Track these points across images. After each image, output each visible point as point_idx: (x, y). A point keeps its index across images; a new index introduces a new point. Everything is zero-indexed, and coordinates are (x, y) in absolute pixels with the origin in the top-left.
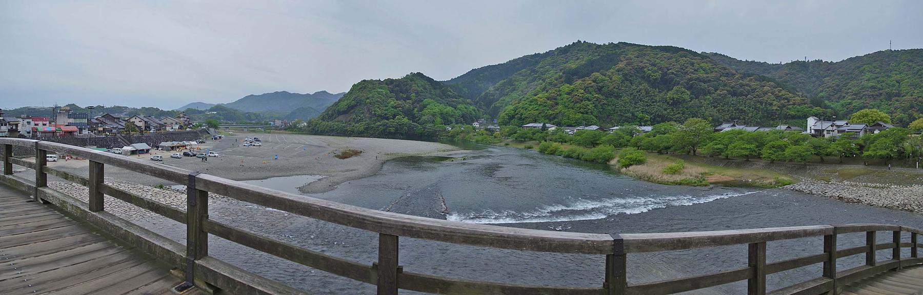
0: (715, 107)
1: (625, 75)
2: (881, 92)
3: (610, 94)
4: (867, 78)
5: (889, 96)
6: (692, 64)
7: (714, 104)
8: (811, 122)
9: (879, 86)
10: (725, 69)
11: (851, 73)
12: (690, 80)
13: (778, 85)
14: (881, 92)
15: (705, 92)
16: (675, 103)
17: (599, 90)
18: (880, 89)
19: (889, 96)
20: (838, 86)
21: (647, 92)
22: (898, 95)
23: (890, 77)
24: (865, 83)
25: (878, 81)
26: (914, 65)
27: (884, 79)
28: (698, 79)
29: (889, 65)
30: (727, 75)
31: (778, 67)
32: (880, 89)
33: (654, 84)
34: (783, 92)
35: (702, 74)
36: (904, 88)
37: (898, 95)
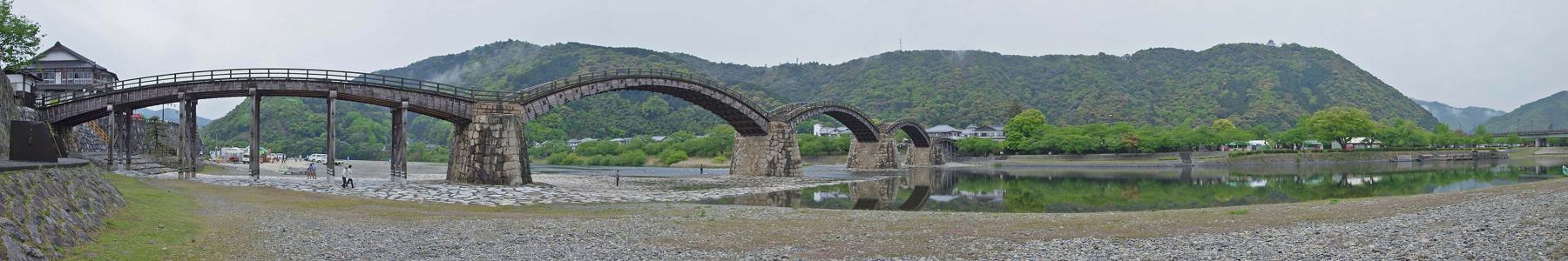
0: (698, 120)
2: (889, 102)
4: (872, 86)
9: (887, 95)
11: (854, 80)
14: (889, 102)
18: (888, 99)
20: (838, 95)
23: (900, 83)
24: (870, 91)
25: (886, 89)
26: (928, 70)
27: (893, 87)
29: (899, 69)
32: (888, 99)
36: (916, 97)
37: (909, 105)
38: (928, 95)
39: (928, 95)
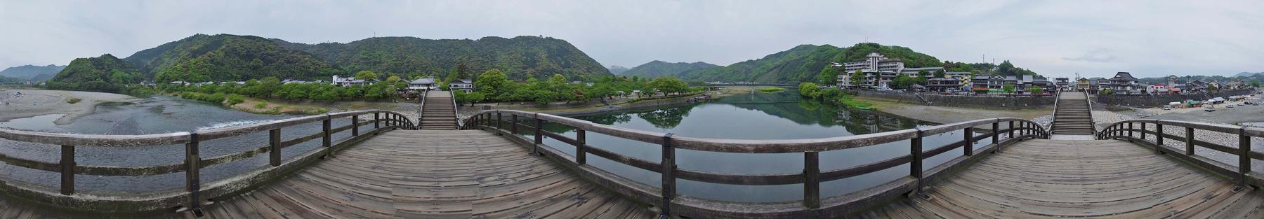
1: (226, 53)
3: (218, 63)
5: (375, 63)
6: (264, 46)
7: (277, 68)
8: (335, 78)
10: (282, 48)
12: (262, 55)
13: (313, 57)
15: (272, 62)
16: (255, 68)
17: (212, 61)
19: (375, 63)
21: (239, 62)
22: (379, 63)
28: (267, 54)
30: (284, 51)
31: (313, 46)
33: (242, 57)
34: (316, 61)
35: (269, 51)
36: (383, 58)
37: (379, 63)
38: (389, 58)
39: (389, 58)
